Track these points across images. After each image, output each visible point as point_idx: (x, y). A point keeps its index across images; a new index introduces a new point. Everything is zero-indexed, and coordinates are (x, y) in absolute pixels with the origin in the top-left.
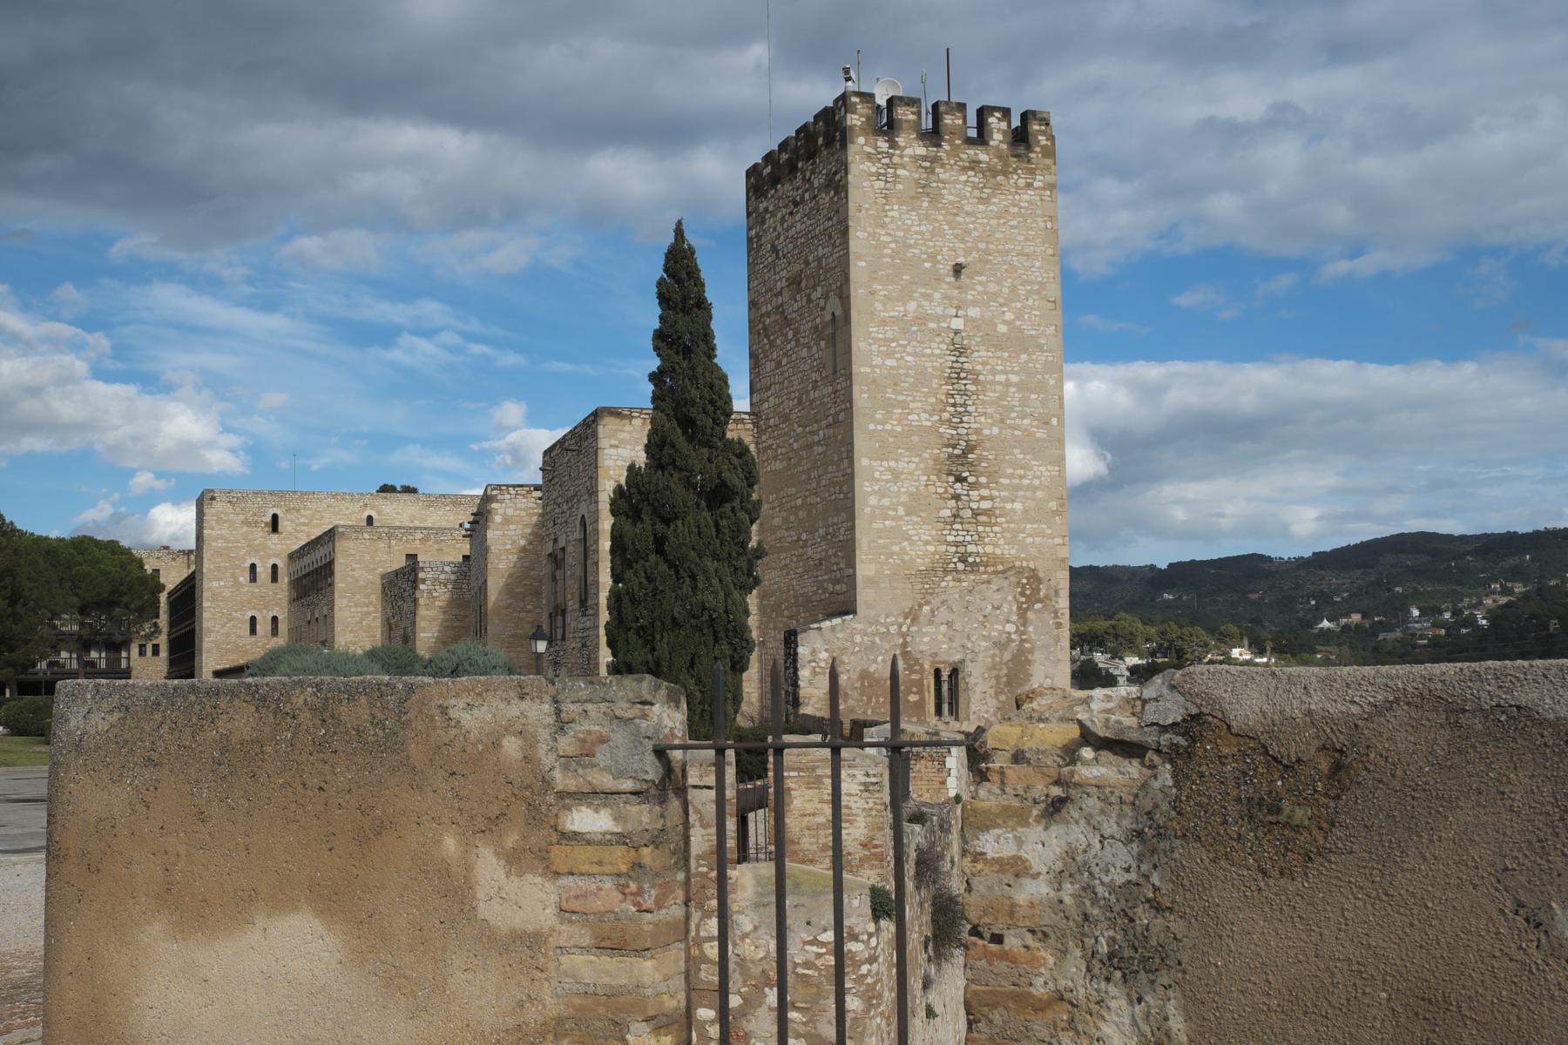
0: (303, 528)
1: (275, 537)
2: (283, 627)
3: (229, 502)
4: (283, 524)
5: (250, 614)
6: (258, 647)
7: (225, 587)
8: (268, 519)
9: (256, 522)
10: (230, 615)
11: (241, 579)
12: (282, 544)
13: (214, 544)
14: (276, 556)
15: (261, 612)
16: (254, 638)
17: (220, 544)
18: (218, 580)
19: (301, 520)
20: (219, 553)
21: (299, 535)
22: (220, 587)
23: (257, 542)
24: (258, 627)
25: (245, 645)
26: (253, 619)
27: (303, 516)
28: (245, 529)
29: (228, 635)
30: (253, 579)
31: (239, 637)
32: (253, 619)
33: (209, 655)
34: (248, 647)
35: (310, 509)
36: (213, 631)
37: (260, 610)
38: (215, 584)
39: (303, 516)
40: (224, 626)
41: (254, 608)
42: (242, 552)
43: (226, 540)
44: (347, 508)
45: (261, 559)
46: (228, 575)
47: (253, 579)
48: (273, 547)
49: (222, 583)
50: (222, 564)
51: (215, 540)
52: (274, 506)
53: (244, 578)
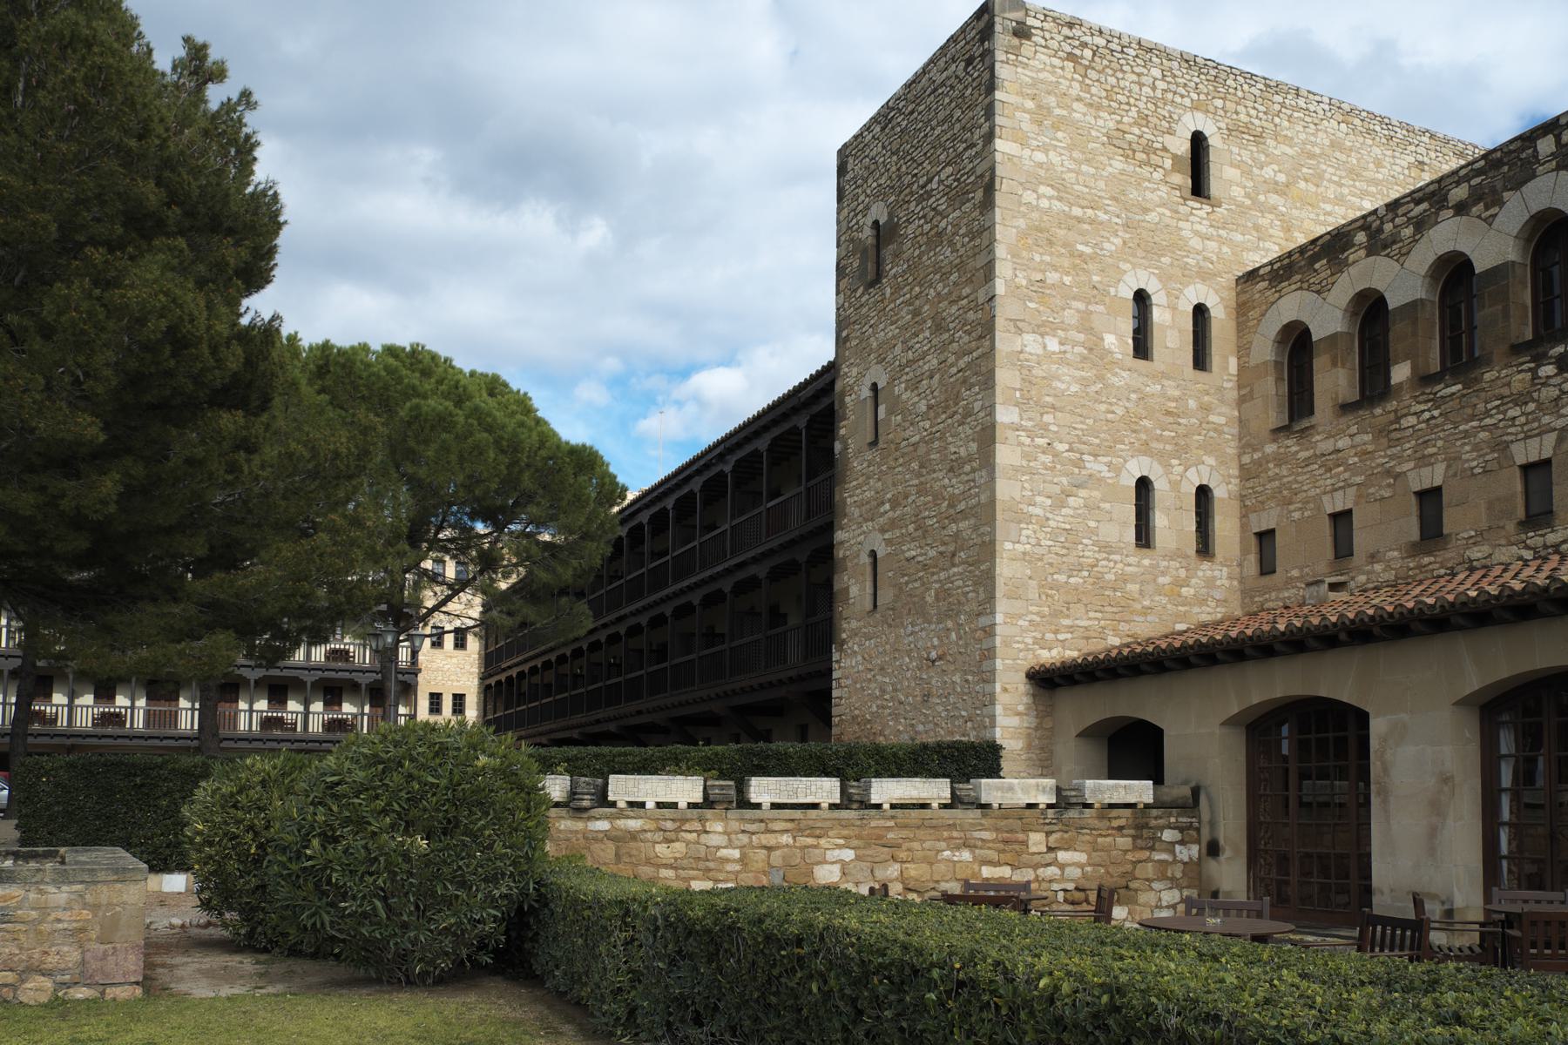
0: (1274, 199)
1: (1200, 209)
2: (1225, 526)
3: (1071, 57)
4: (1221, 173)
5: (1136, 468)
6: (1160, 591)
7: (1062, 358)
8: (1183, 147)
9: (1149, 149)
10: (1080, 464)
11: (1110, 340)
12: (1222, 241)
13: (1029, 197)
14: (1204, 276)
15: (1167, 467)
16: (1146, 560)
17: (1045, 199)
18: (1042, 329)
19: (1268, 172)
20: (1041, 235)
21: (1263, 222)
22: (1049, 355)
23: (1152, 217)
24: (1160, 520)
25: (1124, 579)
26: (1143, 485)
27: (1273, 160)
28: (1118, 164)
29: (1070, 537)
30: (1142, 346)
31: (1106, 548)
32: (1143, 485)
33: (1018, 606)
34: (1133, 588)
35: (1289, 141)
36: (1028, 518)
37: (1162, 458)
38: (1031, 344)
39: (1273, 160)
40: (1059, 503)
41: (1145, 450)
42: (1112, 245)
43: (1061, 189)
44: (1379, 164)
45: (1165, 278)
46: (1070, 317)
47: (1142, 346)
48: (1195, 243)
49: (1053, 345)
50: (1052, 277)
51: (1032, 183)
52: (1196, 107)
53: (1118, 339)
